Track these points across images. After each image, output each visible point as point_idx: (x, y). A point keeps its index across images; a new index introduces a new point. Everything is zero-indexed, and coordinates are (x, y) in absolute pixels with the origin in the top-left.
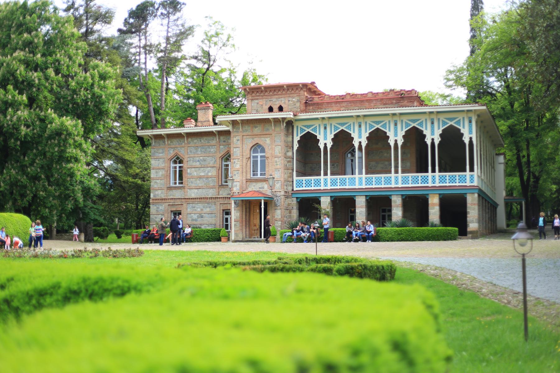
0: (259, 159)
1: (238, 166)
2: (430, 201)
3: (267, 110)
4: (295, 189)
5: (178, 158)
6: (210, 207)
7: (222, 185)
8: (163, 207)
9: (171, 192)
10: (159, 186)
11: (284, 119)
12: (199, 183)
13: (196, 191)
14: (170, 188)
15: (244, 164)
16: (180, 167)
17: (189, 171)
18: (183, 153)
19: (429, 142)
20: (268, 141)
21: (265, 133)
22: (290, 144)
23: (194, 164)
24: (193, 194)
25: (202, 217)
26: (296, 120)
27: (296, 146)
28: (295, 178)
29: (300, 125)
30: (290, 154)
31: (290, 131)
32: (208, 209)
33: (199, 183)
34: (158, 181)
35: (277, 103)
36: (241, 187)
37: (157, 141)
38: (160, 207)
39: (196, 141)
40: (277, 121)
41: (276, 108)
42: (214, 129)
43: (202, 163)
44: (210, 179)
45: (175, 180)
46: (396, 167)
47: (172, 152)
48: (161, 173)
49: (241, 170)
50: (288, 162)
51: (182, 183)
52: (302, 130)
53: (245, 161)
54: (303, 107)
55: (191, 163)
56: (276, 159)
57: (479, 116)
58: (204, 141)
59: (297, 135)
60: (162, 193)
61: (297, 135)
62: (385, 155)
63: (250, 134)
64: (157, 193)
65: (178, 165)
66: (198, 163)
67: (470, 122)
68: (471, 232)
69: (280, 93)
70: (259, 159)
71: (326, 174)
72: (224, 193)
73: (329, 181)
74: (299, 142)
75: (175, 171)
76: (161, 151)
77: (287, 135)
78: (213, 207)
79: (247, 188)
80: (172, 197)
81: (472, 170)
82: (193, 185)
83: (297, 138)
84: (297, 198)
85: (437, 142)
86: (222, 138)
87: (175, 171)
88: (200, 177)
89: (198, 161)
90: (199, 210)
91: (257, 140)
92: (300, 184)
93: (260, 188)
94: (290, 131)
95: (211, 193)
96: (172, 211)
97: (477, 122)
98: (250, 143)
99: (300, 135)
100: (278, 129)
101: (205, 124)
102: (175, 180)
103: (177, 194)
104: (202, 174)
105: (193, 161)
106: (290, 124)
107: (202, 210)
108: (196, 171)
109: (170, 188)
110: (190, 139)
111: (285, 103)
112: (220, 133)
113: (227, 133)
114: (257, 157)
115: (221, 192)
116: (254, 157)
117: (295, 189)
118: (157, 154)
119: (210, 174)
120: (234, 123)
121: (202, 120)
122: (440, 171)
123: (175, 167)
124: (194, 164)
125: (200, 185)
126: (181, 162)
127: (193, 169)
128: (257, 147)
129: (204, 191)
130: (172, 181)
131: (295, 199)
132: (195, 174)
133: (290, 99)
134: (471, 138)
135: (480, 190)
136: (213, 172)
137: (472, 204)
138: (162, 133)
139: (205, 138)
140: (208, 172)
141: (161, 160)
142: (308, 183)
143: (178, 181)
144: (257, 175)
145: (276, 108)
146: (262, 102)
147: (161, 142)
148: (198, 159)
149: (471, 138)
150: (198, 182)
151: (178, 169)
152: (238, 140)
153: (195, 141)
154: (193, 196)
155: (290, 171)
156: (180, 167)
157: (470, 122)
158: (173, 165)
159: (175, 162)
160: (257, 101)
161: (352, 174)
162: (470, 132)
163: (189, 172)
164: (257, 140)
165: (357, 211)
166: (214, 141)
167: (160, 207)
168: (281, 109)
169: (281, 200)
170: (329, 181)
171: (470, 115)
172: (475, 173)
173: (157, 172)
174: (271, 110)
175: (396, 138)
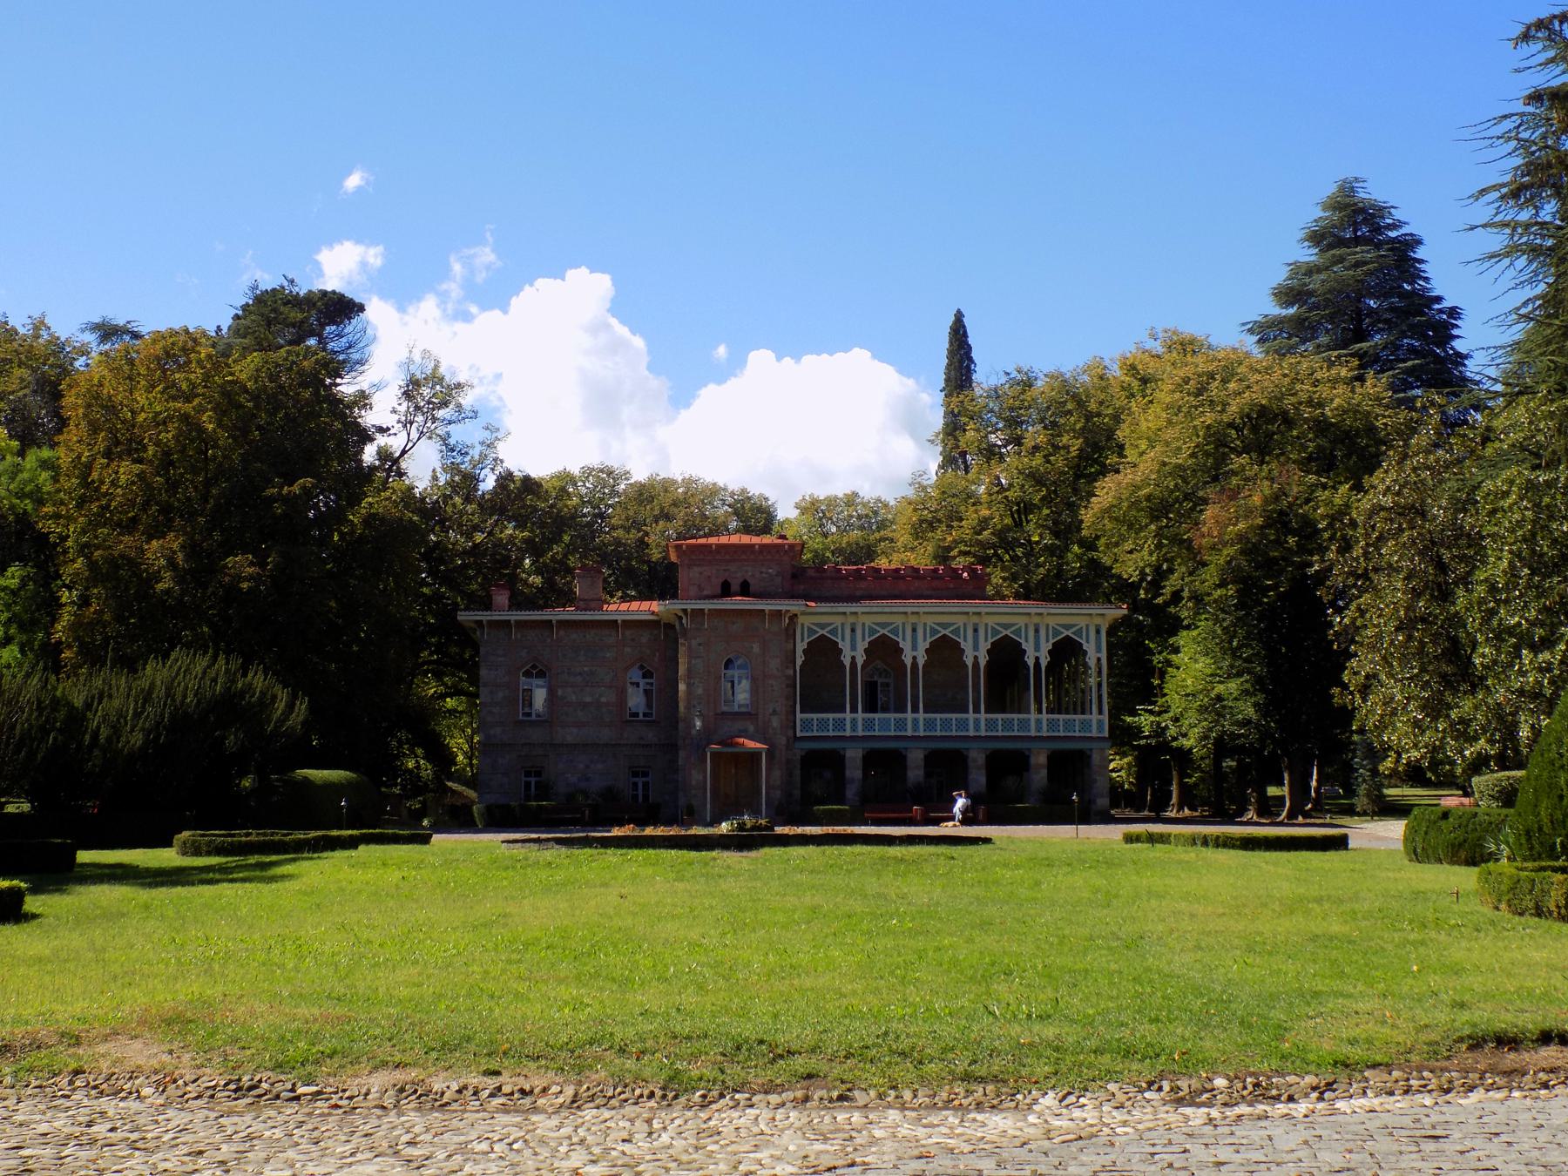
2: (1033, 761)
3: (719, 592)
4: (799, 734)
11: (788, 611)
13: (575, 730)
19: (1031, 662)
24: (570, 735)
28: (799, 715)
30: (791, 672)
32: (600, 766)
41: (735, 587)
48: (501, 695)
73: (860, 723)
83: (801, 647)
88: (585, 705)
90: (581, 766)
92: (807, 725)
101: (593, 605)
104: (588, 699)
107: (587, 767)
110: (562, 633)
111: (753, 576)
117: (799, 734)
119: (603, 700)
122: (864, 711)
134: (1099, 659)
140: (600, 696)
145: (735, 587)
149: (1099, 659)
153: (574, 636)
154: (569, 739)
161: (1083, 713)
162: (1099, 650)
168: (745, 590)
170: (860, 723)
174: (726, 591)
175: (1037, 654)
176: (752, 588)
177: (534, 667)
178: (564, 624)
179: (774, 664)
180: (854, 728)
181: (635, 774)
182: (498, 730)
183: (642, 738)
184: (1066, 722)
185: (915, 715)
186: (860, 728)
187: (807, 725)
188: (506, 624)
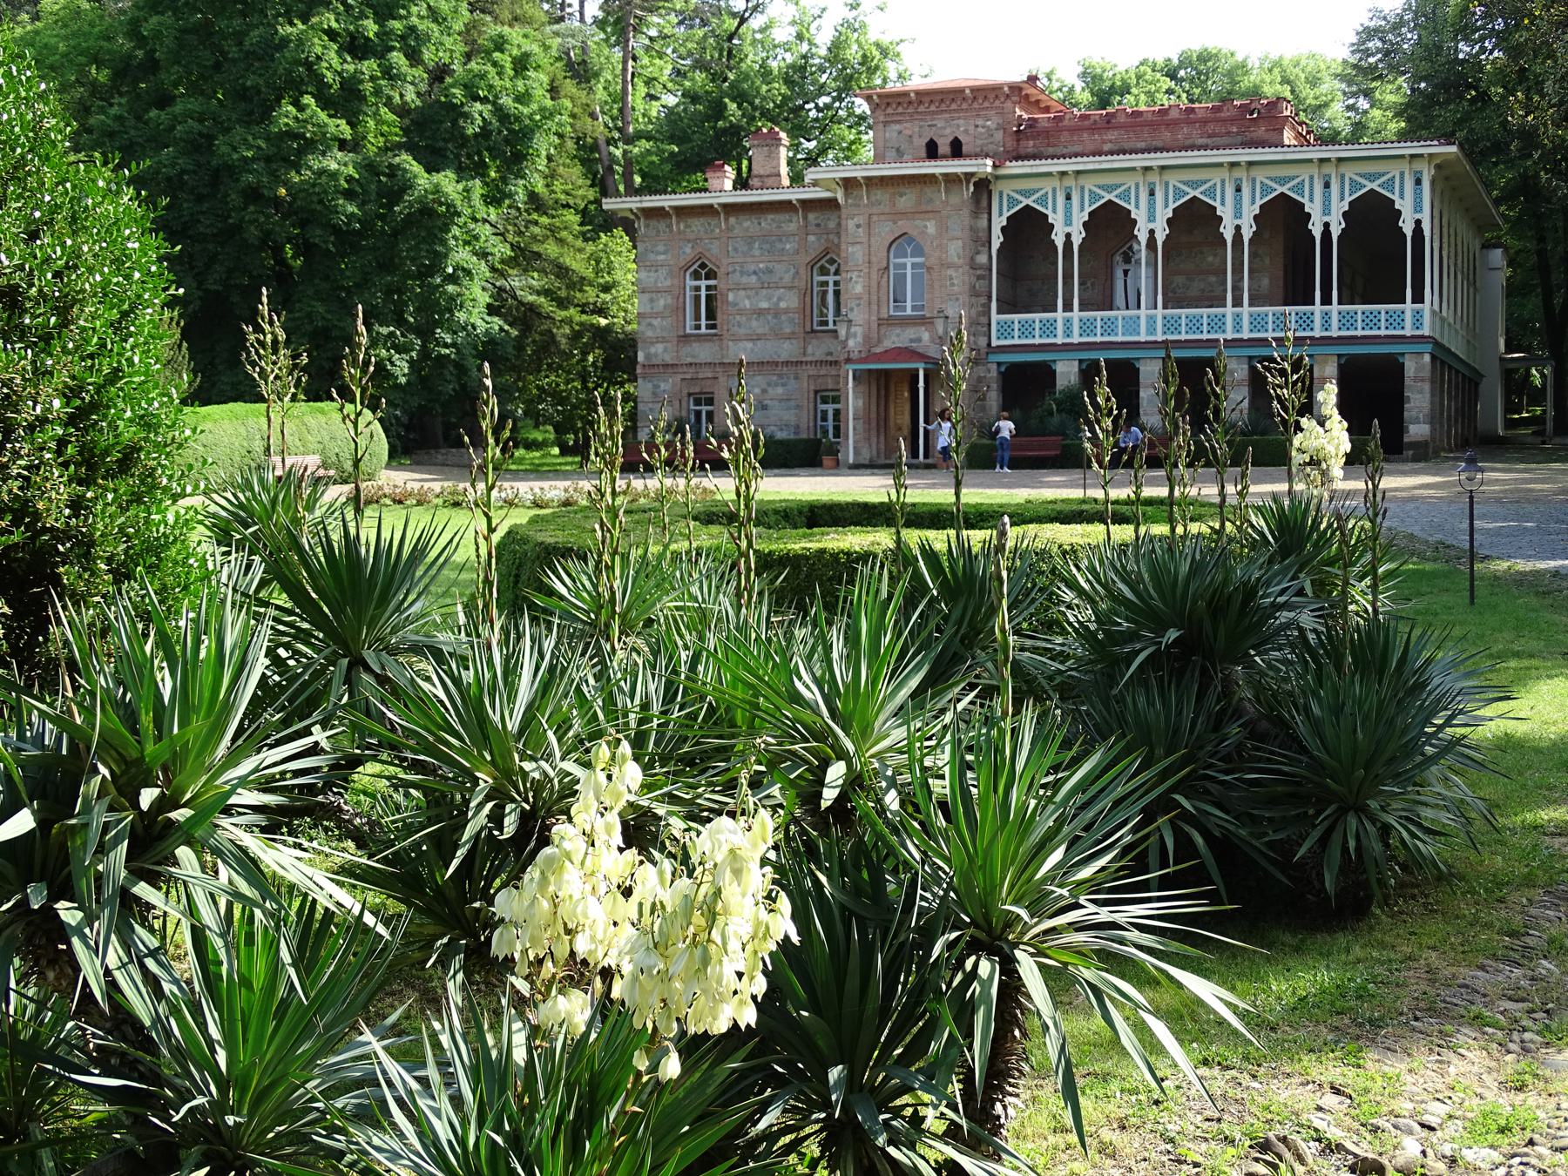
0: (909, 271)
1: (859, 289)
3: (923, 153)
4: (994, 343)
5: (703, 266)
6: (783, 385)
7: (813, 331)
8: (667, 385)
9: (686, 350)
10: (659, 333)
11: (969, 176)
12: (757, 326)
13: (749, 345)
14: (685, 338)
15: (874, 284)
16: (708, 288)
17: (731, 297)
18: (714, 251)
19: (1317, 232)
20: (931, 228)
21: (924, 208)
22: (983, 235)
23: (744, 280)
24: (743, 352)
25: (765, 408)
26: (997, 178)
27: (997, 240)
28: (995, 317)
29: (1007, 188)
30: (983, 259)
31: (984, 203)
32: (780, 390)
33: (757, 326)
34: (656, 322)
35: (948, 131)
36: (867, 338)
37: (653, 223)
38: (662, 385)
39: (748, 224)
40: (951, 180)
41: (944, 148)
42: (795, 195)
43: (765, 278)
44: (783, 317)
45: (698, 318)
46: (1237, 290)
47: (688, 250)
48: (662, 302)
49: (866, 297)
50: (979, 278)
51: (713, 327)
52: (1013, 202)
53: (874, 276)
54: (1011, 144)
55: (736, 277)
56: (950, 272)
57: (1438, 167)
58: (768, 222)
59: (1001, 214)
60: (665, 350)
61: (1001, 214)
62: (1210, 259)
63: (887, 210)
64: (653, 350)
65: (703, 283)
66: (754, 278)
67: (1418, 182)
68: (1415, 445)
69: (954, 106)
70: (909, 271)
71: (1068, 307)
72: (817, 350)
74: (1003, 229)
75: (697, 299)
76: (661, 248)
77: (975, 214)
78: (792, 384)
79: (880, 341)
80: (689, 360)
81: (1418, 298)
82: (742, 331)
83: (999, 222)
84: (999, 364)
85: (1335, 232)
86: (811, 216)
87: (697, 299)
88: (760, 313)
89: (755, 273)
91: (903, 225)
92: (1006, 330)
93: (912, 341)
94: (984, 203)
95: (787, 350)
96: (690, 395)
97: (1433, 183)
98: (885, 231)
99: (1006, 214)
100: (955, 199)
101: (770, 181)
102: (698, 318)
103: (703, 352)
104: (764, 305)
105: (742, 273)
106: (983, 186)
108: (748, 297)
109: (685, 338)
110: (732, 220)
111: (966, 131)
112: (807, 205)
113: (830, 204)
114: (904, 266)
115: (810, 350)
116: (897, 266)
117: (994, 343)
118: (652, 257)
119: (783, 305)
120: (848, 184)
121: (762, 172)
123: (698, 289)
124: (744, 280)
125: (760, 331)
126: (711, 275)
127: (742, 293)
128: (900, 242)
129: (769, 344)
130: (689, 323)
131: (995, 366)
132: (747, 304)
133: (980, 122)
134: (1418, 222)
135: (1437, 344)
136: (790, 301)
137: (1416, 379)
138: (666, 204)
139: (770, 217)
140: (780, 299)
141: (663, 272)
142: (1026, 329)
143: (703, 322)
144: (904, 309)
145: (944, 148)
146: (909, 128)
147: (662, 225)
148: (753, 268)
149: (1418, 222)
150: (754, 323)
151: (703, 293)
152: (858, 226)
153: (746, 224)
155: (983, 300)
156: (708, 288)
157: (1418, 182)
158: (690, 283)
159: (696, 276)
160: (897, 127)
162: (1418, 207)
163: (737, 299)
164: (903, 225)
165: (1142, 394)
166: (793, 224)
167: (662, 385)
168: (957, 150)
169: (958, 368)
171: (1418, 166)
172: (1426, 307)
173: (652, 300)
174: (932, 151)
176: (965, 149)
177: (703, 266)
178: (681, 211)
179: (955, 250)
180: (1068, 332)
181: (825, 401)
182: (660, 348)
183: (830, 354)
184: (1113, 332)
185: (1068, 314)
186: (1076, 330)
187: (1006, 330)
188: (785, 206)
